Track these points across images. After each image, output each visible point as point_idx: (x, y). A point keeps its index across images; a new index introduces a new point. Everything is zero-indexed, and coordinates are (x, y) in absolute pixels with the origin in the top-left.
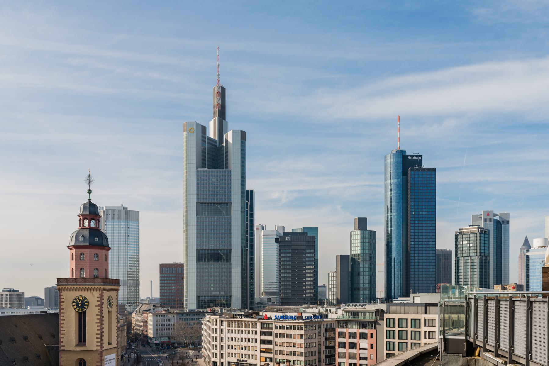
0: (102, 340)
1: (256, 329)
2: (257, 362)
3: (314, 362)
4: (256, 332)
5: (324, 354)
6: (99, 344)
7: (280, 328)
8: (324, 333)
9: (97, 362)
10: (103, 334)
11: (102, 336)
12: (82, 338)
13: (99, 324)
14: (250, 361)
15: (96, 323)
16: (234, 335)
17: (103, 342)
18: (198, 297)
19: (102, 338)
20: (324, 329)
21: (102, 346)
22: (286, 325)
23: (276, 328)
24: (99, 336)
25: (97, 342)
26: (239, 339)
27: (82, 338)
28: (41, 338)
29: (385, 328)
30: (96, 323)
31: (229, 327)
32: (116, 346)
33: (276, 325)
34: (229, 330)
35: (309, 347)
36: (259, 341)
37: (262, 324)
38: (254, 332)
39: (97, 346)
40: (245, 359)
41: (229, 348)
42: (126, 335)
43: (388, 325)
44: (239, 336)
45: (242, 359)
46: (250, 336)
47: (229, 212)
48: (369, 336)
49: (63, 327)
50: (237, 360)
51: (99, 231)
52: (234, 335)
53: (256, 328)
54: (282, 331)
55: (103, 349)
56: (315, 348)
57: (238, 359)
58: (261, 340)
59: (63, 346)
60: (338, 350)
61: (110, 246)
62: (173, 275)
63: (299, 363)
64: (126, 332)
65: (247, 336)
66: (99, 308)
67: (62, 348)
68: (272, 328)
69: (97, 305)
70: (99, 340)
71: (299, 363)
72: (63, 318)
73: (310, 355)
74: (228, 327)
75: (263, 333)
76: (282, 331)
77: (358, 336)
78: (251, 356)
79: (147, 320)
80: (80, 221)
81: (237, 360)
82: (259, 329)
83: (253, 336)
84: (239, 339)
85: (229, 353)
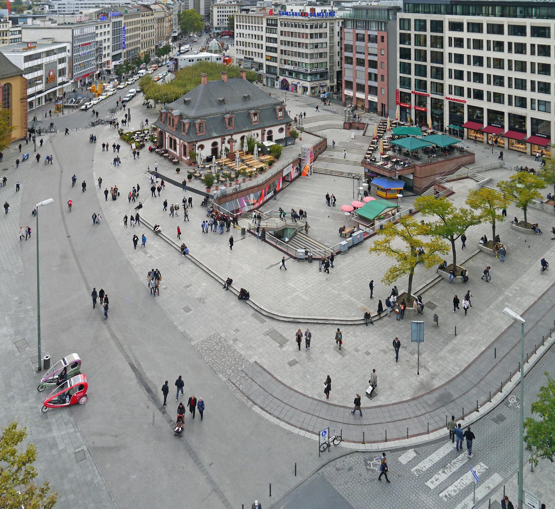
2: (263, 61)
3: (324, 65)
8: (338, 32)
14: (257, 59)
29: (399, 31)
35: (316, 47)
40: (252, 57)
43: (402, 26)
45: (249, 57)
48: (379, 39)
50: (245, 57)
57: (246, 56)
63: (304, 65)
71: (304, 65)
77: (366, 38)
78: (257, 54)
81: (245, 57)
85: (237, 50)
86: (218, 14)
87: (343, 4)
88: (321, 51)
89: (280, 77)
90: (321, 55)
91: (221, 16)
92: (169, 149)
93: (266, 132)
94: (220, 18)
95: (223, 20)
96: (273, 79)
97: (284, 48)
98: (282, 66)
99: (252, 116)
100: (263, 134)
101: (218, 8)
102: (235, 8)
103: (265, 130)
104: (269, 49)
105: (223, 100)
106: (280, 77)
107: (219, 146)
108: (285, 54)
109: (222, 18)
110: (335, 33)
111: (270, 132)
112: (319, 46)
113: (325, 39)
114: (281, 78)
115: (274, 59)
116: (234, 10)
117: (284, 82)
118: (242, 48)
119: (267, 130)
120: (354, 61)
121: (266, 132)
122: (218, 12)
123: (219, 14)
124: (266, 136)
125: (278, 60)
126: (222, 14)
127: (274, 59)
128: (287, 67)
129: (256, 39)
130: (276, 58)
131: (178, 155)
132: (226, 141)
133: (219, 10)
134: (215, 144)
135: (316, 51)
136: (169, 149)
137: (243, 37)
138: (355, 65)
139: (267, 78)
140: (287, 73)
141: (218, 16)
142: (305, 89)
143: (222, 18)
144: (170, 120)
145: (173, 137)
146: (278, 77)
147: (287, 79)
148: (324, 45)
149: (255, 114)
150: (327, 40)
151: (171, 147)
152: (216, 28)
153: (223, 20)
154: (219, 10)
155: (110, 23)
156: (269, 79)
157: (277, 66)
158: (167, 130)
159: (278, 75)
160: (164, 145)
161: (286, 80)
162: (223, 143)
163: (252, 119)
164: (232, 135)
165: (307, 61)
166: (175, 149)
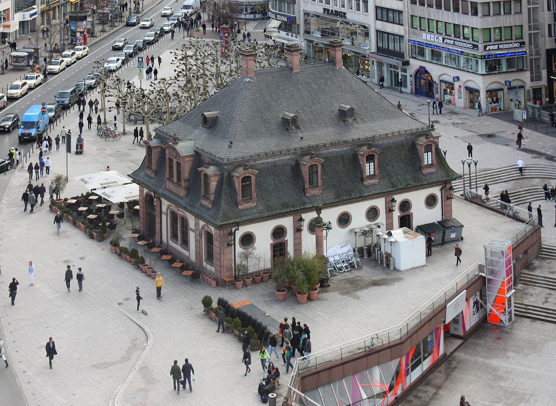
5: (549, 9)
40: (342, 10)
45: (335, 8)
50: (325, 10)
57: (327, 7)
89: (412, 61)
92: (171, 243)
93: (397, 205)
96: (395, 67)
98: (415, 34)
99: (363, 160)
100: (390, 211)
103: (393, 200)
105: (294, 120)
106: (412, 61)
107: (289, 237)
111: (405, 205)
114: (415, 64)
117: (422, 71)
119: (399, 198)
121: (397, 205)
124: (397, 214)
125: (406, 18)
128: (426, 37)
131: (193, 258)
132: (305, 225)
134: (279, 232)
136: (171, 243)
139: (380, 64)
140: (428, 52)
142: (472, 92)
144: (171, 167)
145: (181, 212)
146: (407, 63)
147: (429, 67)
149: (370, 158)
151: (174, 236)
156: (385, 68)
157: (402, 33)
158: (167, 193)
159: (407, 58)
160: (157, 230)
161: (427, 72)
162: (298, 230)
163: (362, 171)
164: (319, 210)
166: (185, 243)
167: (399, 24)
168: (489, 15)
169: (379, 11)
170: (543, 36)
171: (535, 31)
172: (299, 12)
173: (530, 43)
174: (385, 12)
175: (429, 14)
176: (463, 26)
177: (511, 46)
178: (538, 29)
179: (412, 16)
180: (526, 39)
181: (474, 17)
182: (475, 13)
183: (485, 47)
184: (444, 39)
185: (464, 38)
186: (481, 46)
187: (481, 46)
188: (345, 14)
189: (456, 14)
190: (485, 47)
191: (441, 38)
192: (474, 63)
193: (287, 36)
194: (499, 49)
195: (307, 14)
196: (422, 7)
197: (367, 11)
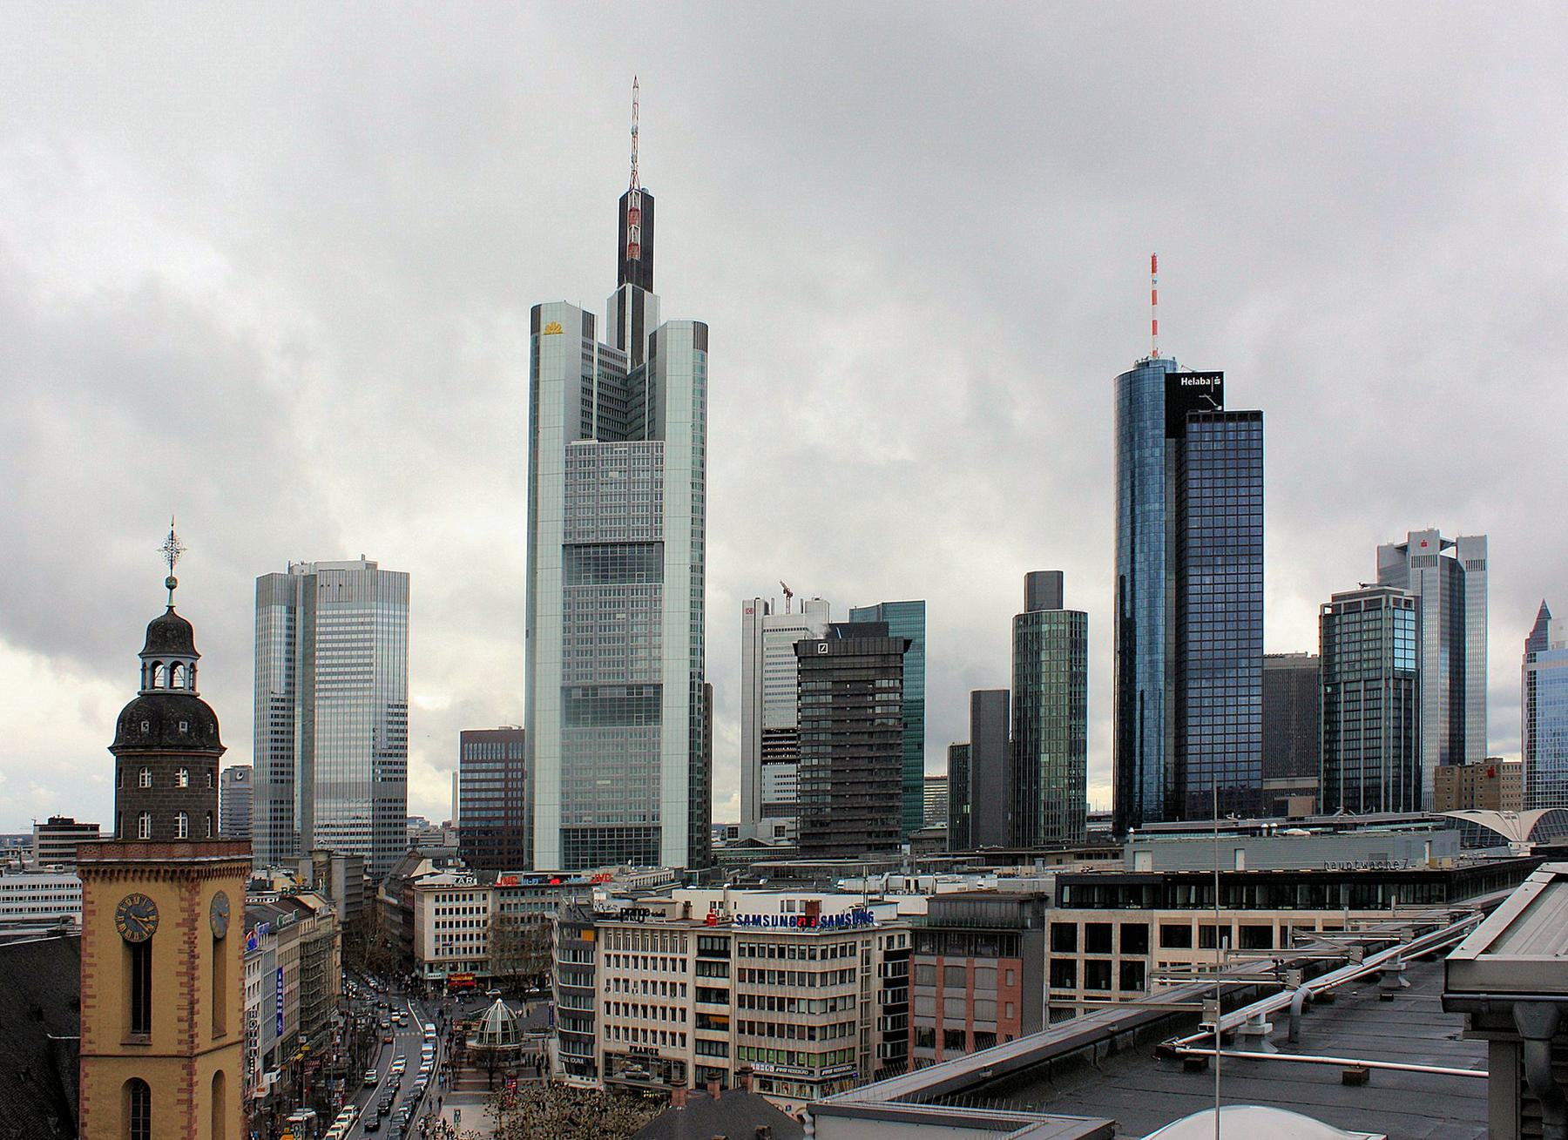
0: (192, 1025)
1: (683, 956)
2: (688, 1055)
4: (684, 961)
6: (186, 1036)
7: (752, 952)
9: (180, 1090)
10: (197, 1007)
11: (192, 1012)
12: (140, 1016)
13: (185, 979)
14: (668, 1052)
15: (178, 974)
16: (623, 973)
17: (196, 1030)
18: (565, 832)
19: (192, 1019)
20: (882, 951)
21: (193, 1042)
22: (769, 945)
23: (741, 951)
24: (184, 1014)
25: (180, 1031)
26: (636, 983)
27: (140, 1016)
28: (39, 1014)
30: (178, 974)
31: (608, 947)
32: (241, 1038)
33: (739, 943)
34: (608, 956)
35: (833, 1009)
36: (691, 991)
37: (699, 937)
38: (679, 965)
39: (180, 1042)
40: (654, 1046)
41: (608, 1012)
42: (339, 963)
44: (636, 975)
46: (668, 976)
47: (655, 572)
49: (91, 987)
51: (195, 697)
52: (623, 973)
53: (683, 950)
54: (757, 963)
55: (196, 1051)
56: (852, 1011)
57: (634, 1044)
58: (697, 988)
59: (90, 1042)
60: (913, 1021)
61: (223, 743)
62: (499, 766)
64: (339, 954)
65: (660, 976)
66: (186, 930)
67: (88, 1047)
68: (727, 954)
69: (181, 921)
70: (185, 1026)
72: (94, 960)
73: (837, 1036)
74: (606, 948)
75: (702, 968)
76: (757, 963)
79: (412, 907)
80: (144, 670)
81: (631, 1048)
82: (692, 955)
83: (678, 977)
84: (636, 983)
86: (437, 918)
87: (841, 882)
88: (843, 1017)
90: (843, 1028)
91: (451, 924)
94: (441, 931)
95: (451, 937)
97: (746, 1015)
101: (437, 900)
102: (485, 897)
104: (703, 1021)
108: (751, 1032)
109: (448, 931)
110: (872, 970)
112: (840, 1005)
113: (851, 985)
115: (720, 1048)
116: (481, 904)
118: (621, 1021)
120: (939, 1037)
122: (437, 912)
123: (441, 918)
125: (732, 1049)
126: (448, 918)
127: (720, 1048)
129: (664, 993)
130: (725, 1044)
133: (441, 905)
135: (833, 1019)
137: (627, 990)
138: (942, 1047)
141: (437, 925)
143: (448, 931)
148: (849, 1002)
150: (855, 989)
152: (431, 965)
153: (451, 937)
154: (441, 905)
155: (260, 958)
165: (814, 1047)
167: (723, 1056)
168: (826, 1038)
169: (700, 1044)
170: (873, 1057)
171: (866, 1053)
172: (599, 1052)
173: (861, 1066)
174: (707, 1045)
175: (760, 1043)
176: (798, 1053)
177: (844, 1069)
178: (868, 1050)
179: (739, 1047)
180: (858, 1062)
181: (812, 1042)
182: (812, 1038)
183: (821, 1072)
184: (775, 1068)
185: (799, 1065)
186: (817, 1072)
187: (817, 1072)
188: (657, 1050)
189: (791, 1040)
190: (821, 1072)
191: (772, 1067)
192: (808, 1089)
193: (581, 1081)
194: (833, 1073)
195: (608, 1054)
196: (751, 1036)
197: (684, 1045)
